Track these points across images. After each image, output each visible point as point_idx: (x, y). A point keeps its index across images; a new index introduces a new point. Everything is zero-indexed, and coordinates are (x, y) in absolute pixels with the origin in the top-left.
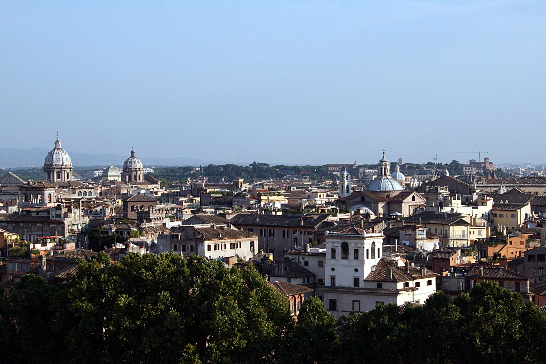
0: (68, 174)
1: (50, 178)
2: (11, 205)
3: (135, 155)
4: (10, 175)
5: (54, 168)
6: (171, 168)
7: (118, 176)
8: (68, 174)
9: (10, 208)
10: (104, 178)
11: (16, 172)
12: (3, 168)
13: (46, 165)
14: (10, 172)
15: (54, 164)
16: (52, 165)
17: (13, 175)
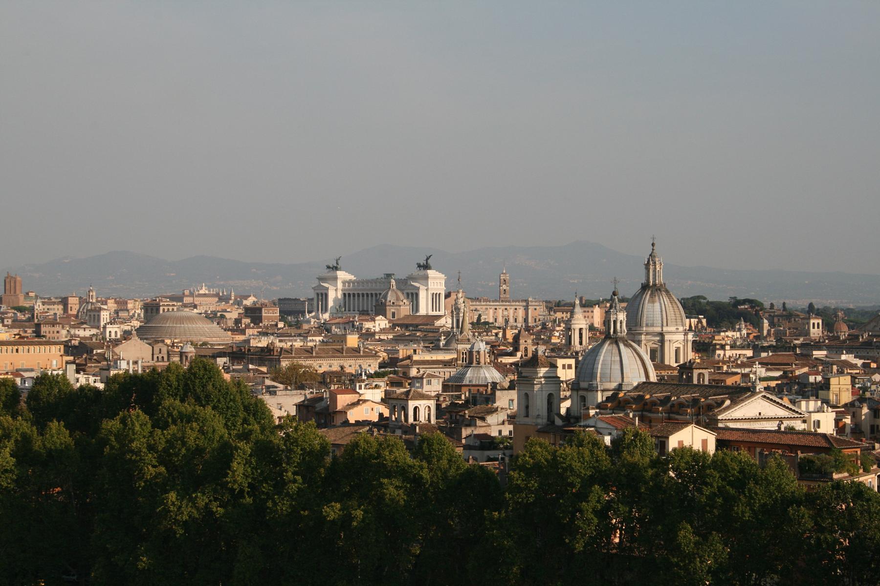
12: (851, 306)
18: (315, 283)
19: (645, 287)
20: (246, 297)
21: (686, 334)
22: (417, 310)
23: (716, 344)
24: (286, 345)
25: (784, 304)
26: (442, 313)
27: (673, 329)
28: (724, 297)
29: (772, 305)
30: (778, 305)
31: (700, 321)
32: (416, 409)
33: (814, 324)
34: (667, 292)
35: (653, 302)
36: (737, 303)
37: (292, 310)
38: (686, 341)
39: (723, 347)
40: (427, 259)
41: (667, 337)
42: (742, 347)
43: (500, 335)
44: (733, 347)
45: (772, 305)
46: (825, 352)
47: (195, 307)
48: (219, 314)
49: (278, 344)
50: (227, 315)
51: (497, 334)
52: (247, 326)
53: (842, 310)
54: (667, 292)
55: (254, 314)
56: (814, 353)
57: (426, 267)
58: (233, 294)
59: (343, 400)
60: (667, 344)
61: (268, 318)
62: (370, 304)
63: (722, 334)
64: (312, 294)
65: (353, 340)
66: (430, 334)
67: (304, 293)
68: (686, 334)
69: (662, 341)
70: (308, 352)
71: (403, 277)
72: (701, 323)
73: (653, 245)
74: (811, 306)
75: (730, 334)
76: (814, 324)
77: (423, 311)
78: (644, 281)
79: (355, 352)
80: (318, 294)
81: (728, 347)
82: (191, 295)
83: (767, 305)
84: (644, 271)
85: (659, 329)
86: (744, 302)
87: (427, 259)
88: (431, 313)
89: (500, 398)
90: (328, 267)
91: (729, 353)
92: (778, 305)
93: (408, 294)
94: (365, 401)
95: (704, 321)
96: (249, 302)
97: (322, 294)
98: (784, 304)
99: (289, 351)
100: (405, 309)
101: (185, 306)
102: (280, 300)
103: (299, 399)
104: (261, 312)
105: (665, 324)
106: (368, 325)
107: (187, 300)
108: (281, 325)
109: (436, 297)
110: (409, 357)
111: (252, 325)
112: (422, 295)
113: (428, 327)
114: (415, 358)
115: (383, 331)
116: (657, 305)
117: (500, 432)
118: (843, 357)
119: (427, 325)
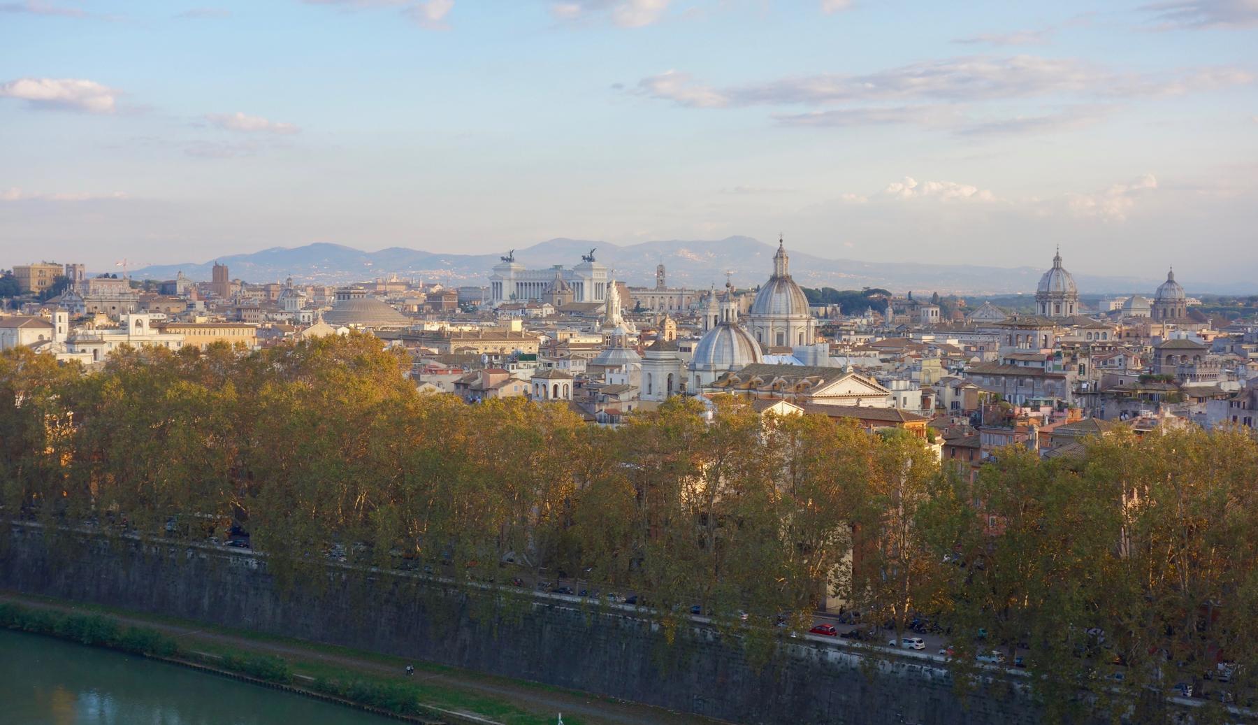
18: (492, 273)
19: (774, 279)
20: (433, 286)
21: (809, 320)
24: (454, 329)
28: (858, 288)
32: (556, 387)
34: (793, 283)
38: (808, 327)
41: (792, 323)
42: (866, 333)
47: (385, 294)
49: (448, 328)
52: (428, 312)
57: (591, 259)
59: (495, 378)
60: (791, 330)
61: (448, 305)
62: (538, 293)
65: (517, 325)
68: (809, 320)
69: (788, 328)
70: (474, 336)
75: (858, 320)
78: (772, 272)
79: (517, 336)
82: (384, 284)
85: (784, 316)
88: (594, 301)
91: (853, 338)
94: (515, 380)
96: (434, 290)
99: (457, 336)
100: (569, 299)
101: (376, 293)
103: (457, 378)
106: (535, 312)
107: (380, 288)
108: (458, 311)
110: (566, 341)
112: (586, 284)
114: (572, 341)
115: (550, 317)
116: (783, 295)
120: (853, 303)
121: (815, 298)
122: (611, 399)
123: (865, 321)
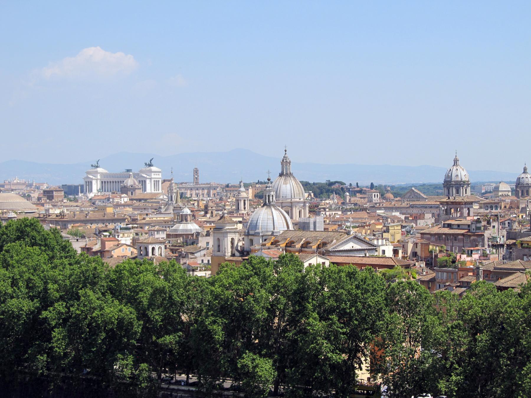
0: (466, 190)
1: (449, 193)
2: (420, 219)
3: (528, 171)
4: (413, 191)
5: (453, 184)
6: (434, 185)
7: (508, 191)
8: (466, 190)
9: (419, 221)
10: (496, 193)
11: (416, 187)
13: (445, 181)
14: (413, 188)
15: (453, 180)
16: (451, 181)
17: (416, 191)
18: (85, 175)
19: (281, 175)
22: (145, 191)
23: (320, 209)
25: (357, 184)
26: (160, 191)
27: (298, 200)
28: (323, 180)
29: (351, 185)
30: (354, 185)
31: (310, 195)
32: (153, 249)
33: (375, 195)
34: (294, 177)
35: (286, 184)
36: (331, 184)
37: (71, 191)
39: (324, 209)
40: (151, 160)
42: (336, 210)
43: (196, 204)
44: (330, 210)
45: (351, 185)
46: (383, 211)
48: (27, 195)
50: (32, 195)
51: (193, 204)
53: (389, 186)
54: (294, 177)
55: (49, 194)
56: (377, 211)
58: (34, 183)
61: (58, 197)
63: (323, 202)
64: (83, 182)
66: (154, 204)
67: (77, 181)
71: (137, 172)
72: (311, 195)
73: (286, 151)
74: (372, 184)
75: (327, 201)
76: (375, 195)
77: (148, 190)
80: (86, 182)
81: (327, 210)
83: (348, 184)
84: (280, 166)
85: (289, 200)
86: (336, 182)
87: (151, 160)
88: (153, 191)
89: (201, 241)
90: (92, 166)
92: (354, 185)
93: (140, 181)
95: (312, 194)
96: (45, 187)
97: (89, 182)
98: (357, 184)
102: (63, 185)
104: (53, 193)
105: (293, 197)
109: (156, 182)
111: (48, 201)
112: (148, 181)
113: (153, 200)
116: (288, 185)
117: (202, 261)
118: (394, 214)
119: (152, 199)
120: (321, 190)
121: (306, 186)
122: (190, 256)
123: (331, 202)
